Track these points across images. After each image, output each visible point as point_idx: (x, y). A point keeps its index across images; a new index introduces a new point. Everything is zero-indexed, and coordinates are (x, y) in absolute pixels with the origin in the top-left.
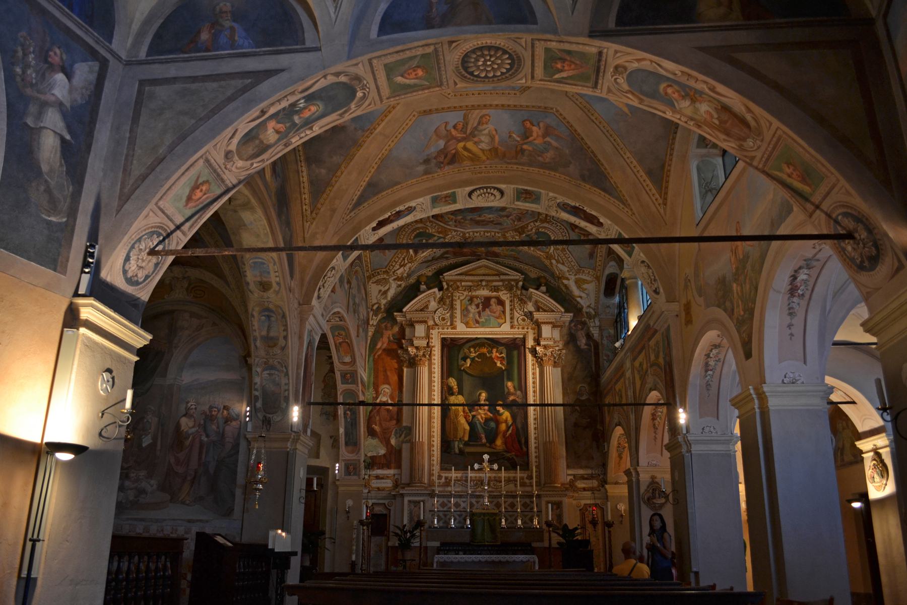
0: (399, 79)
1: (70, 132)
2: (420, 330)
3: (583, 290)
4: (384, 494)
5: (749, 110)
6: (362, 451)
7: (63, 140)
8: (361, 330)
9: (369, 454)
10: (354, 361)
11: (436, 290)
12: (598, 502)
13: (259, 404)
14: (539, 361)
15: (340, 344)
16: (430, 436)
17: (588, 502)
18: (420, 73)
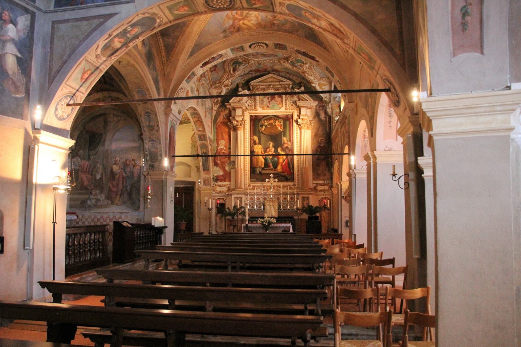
0: (176, 12)
2: (239, 112)
4: (224, 194)
5: (341, 26)
6: (211, 174)
7: (18, 58)
8: (207, 113)
9: (215, 175)
10: (204, 130)
12: (328, 196)
13: (148, 158)
15: (196, 121)
18: (186, 8)
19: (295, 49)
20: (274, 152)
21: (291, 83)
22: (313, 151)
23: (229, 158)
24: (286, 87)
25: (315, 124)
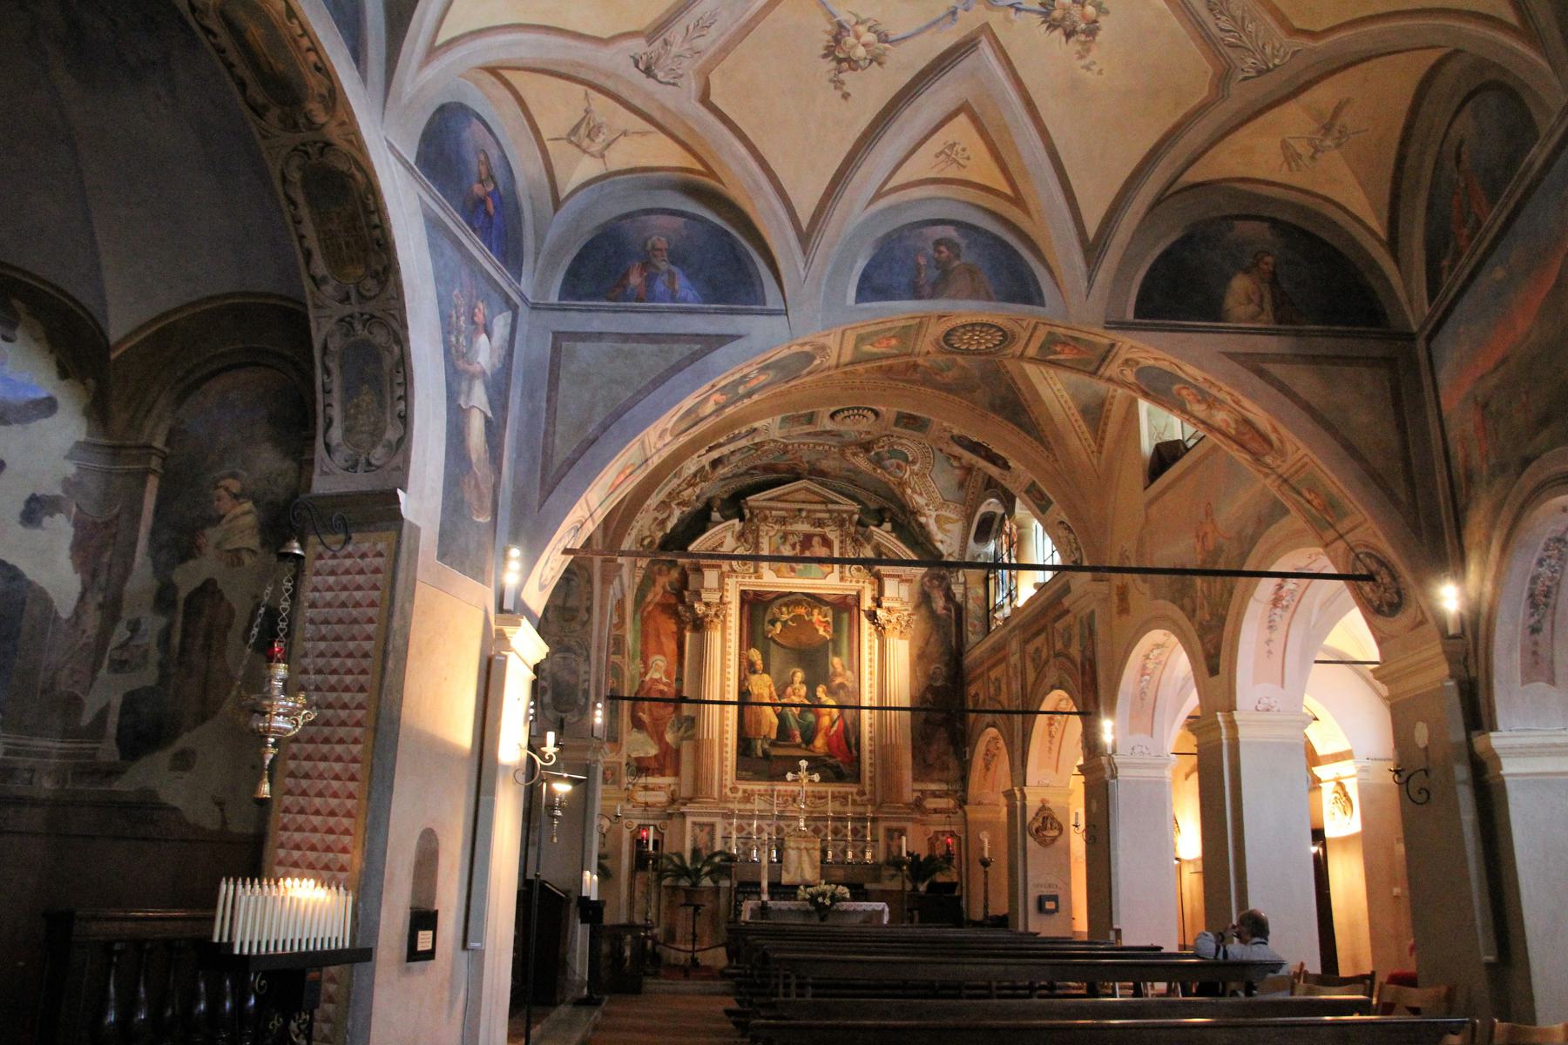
1: (492, 408)
2: (711, 578)
3: (945, 531)
4: (656, 811)
5: (1275, 430)
6: (624, 750)
7: (486, 417)
11: (736, 521)
12: (954, 828)
13: (547, 699)
14: (880, 630)
16: (722, 732)
17: (941, 828)
18: (893, 342)
19: (956, 432)
20: (807, 697)
21: (856, 507)
22: (912, 698)
23: (677, 709)
24: (844, 520)
25: (918, 624)
